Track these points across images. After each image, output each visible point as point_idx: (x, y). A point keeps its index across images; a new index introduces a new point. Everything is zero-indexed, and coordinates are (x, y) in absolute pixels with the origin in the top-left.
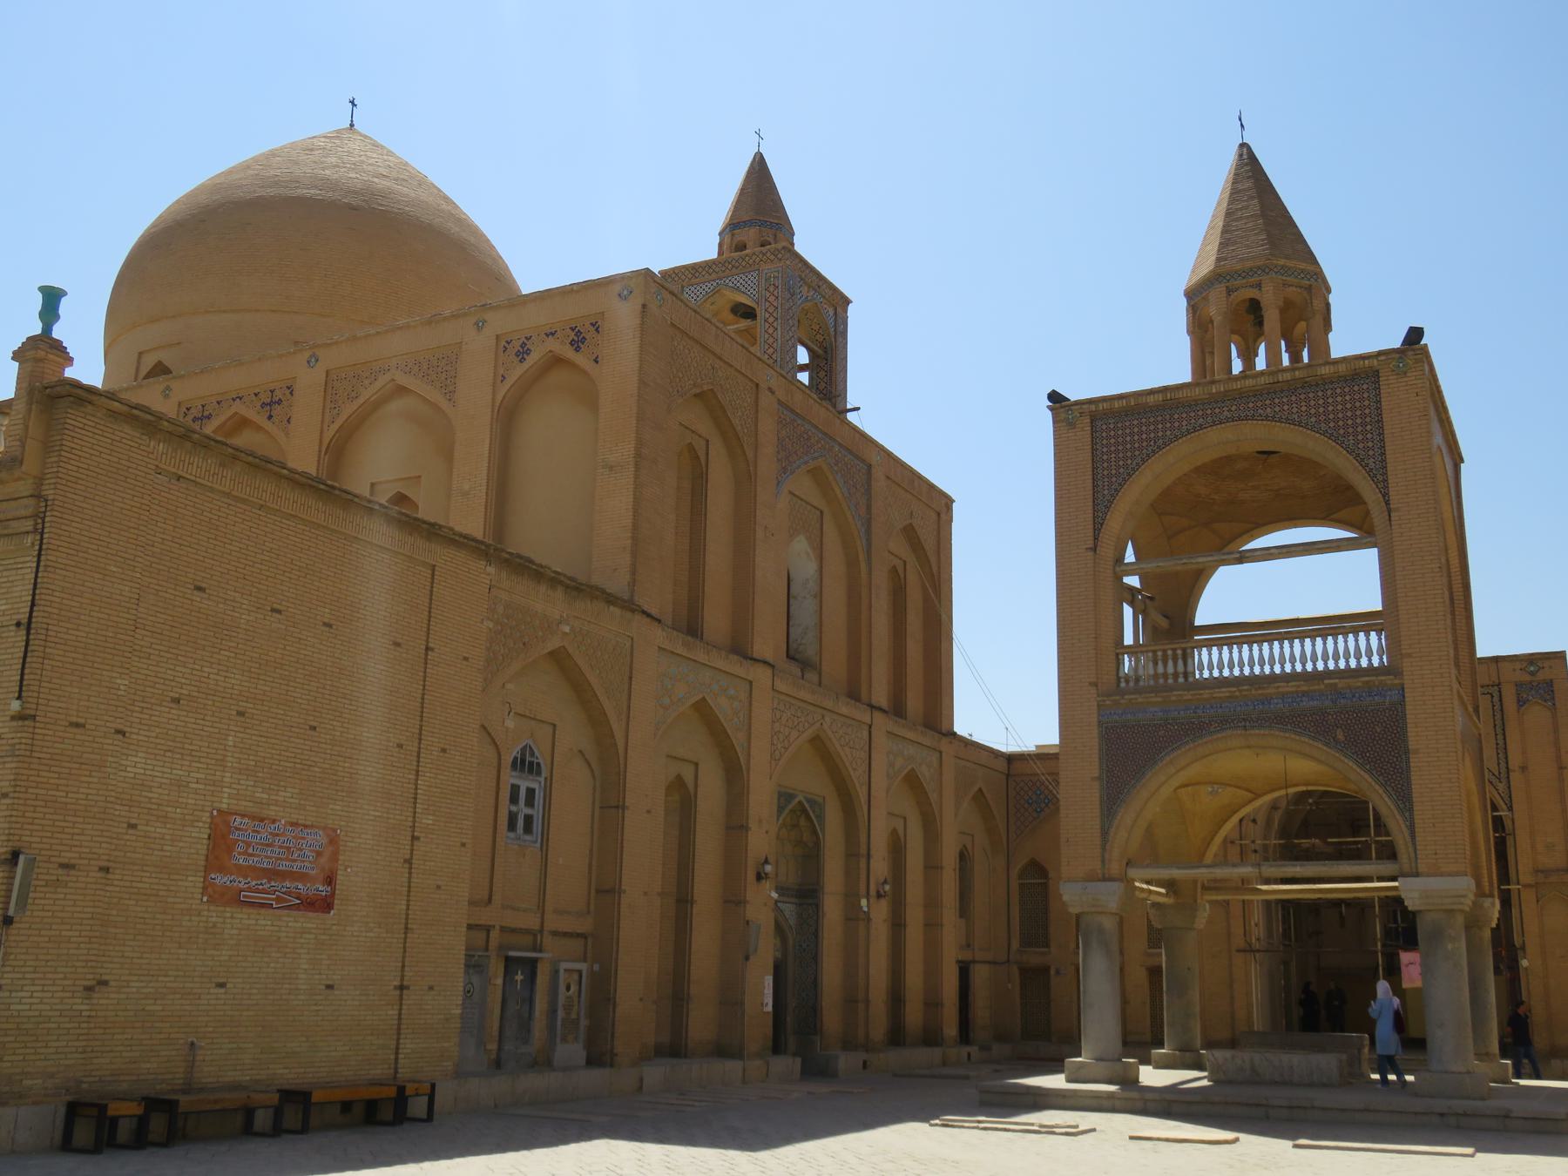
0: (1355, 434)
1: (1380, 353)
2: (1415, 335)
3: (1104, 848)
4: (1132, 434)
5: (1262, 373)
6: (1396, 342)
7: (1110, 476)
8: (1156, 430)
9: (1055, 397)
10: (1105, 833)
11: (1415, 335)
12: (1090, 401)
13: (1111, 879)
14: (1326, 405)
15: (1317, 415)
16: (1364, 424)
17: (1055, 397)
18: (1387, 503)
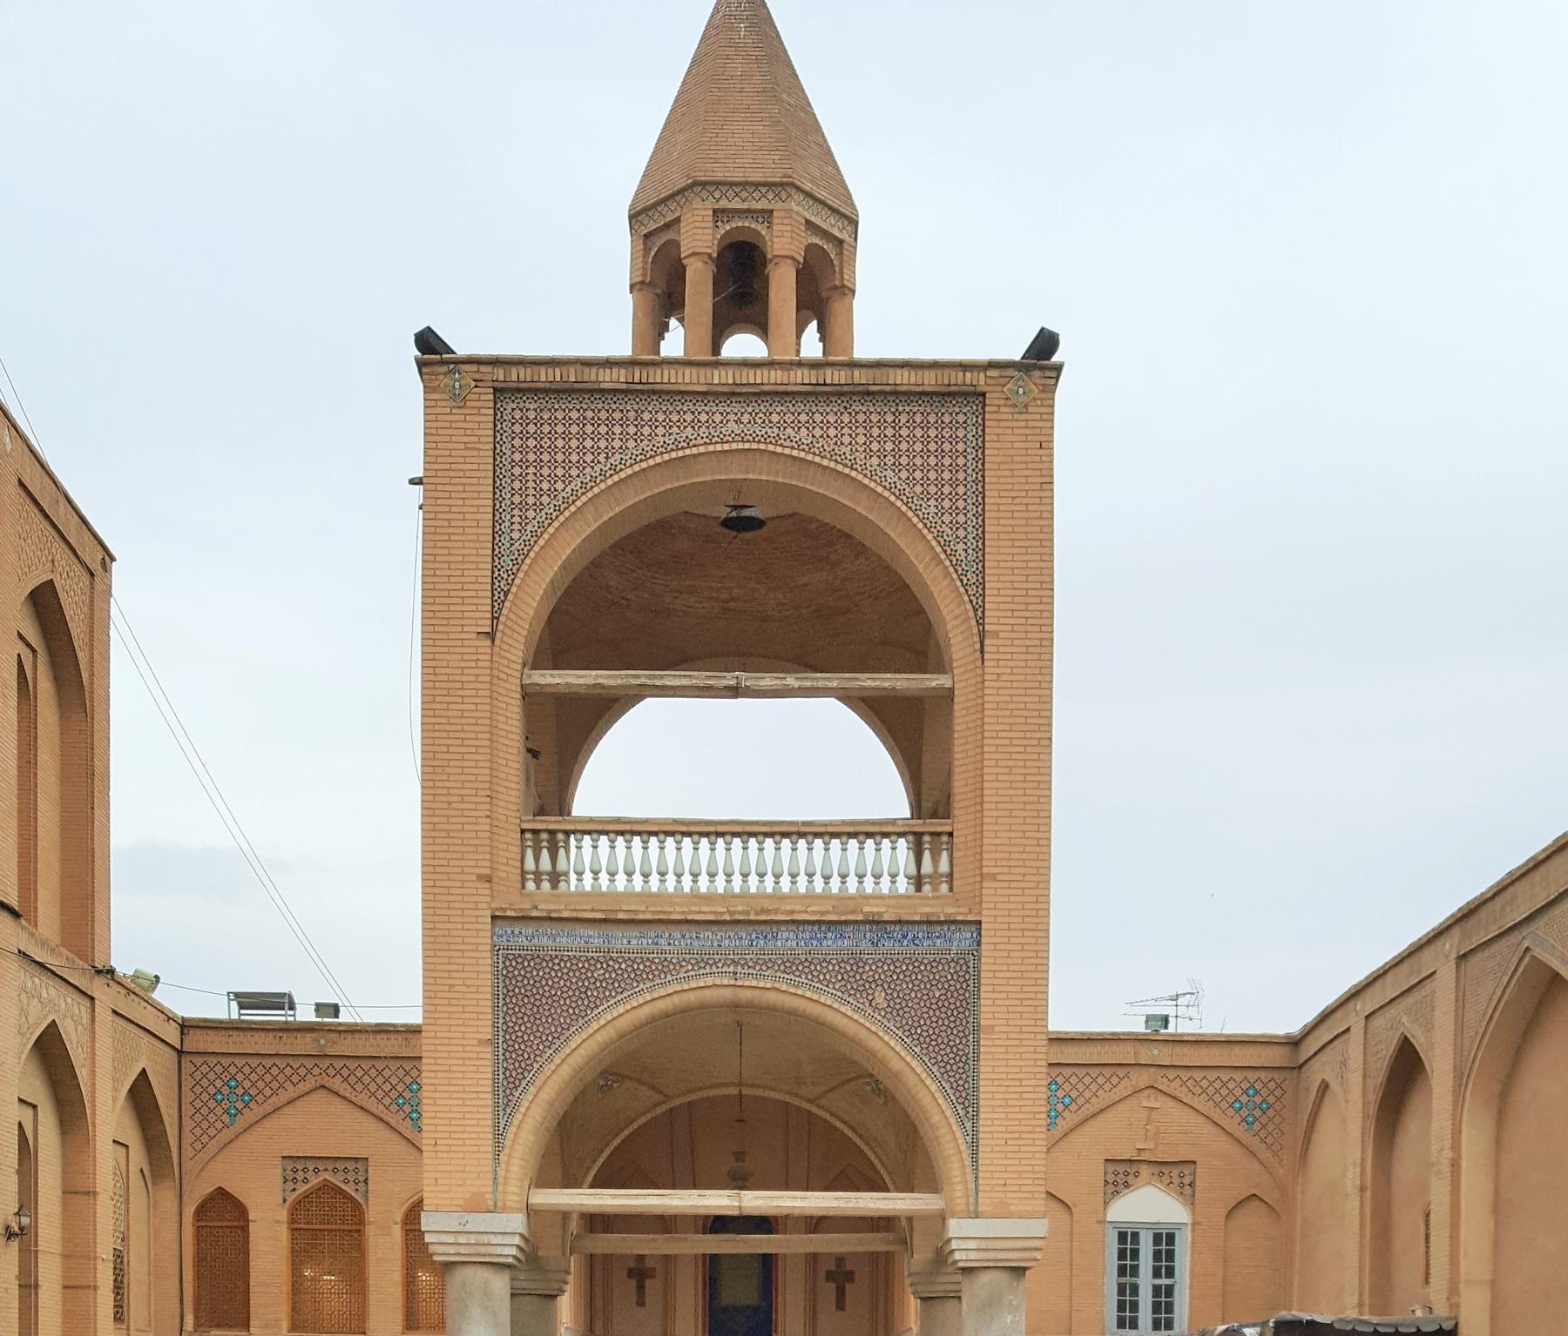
0: (940, 497)
1: (992, 365)
2: (1045, 344)
3: (496, 1159)
4: (566, 436)
5: (814, 365)
6: (1015, 351)
7: (523, 507)
8: (609, 435)
9: (428, 342)
10: (499, 1136)
11: (1045, 344)
12: (496, 362)
13: (505, 1209)
14: (897, 439)
15: (882, 454)
16: (954, 483)
17: (428, 342)
18: (981, 622)
